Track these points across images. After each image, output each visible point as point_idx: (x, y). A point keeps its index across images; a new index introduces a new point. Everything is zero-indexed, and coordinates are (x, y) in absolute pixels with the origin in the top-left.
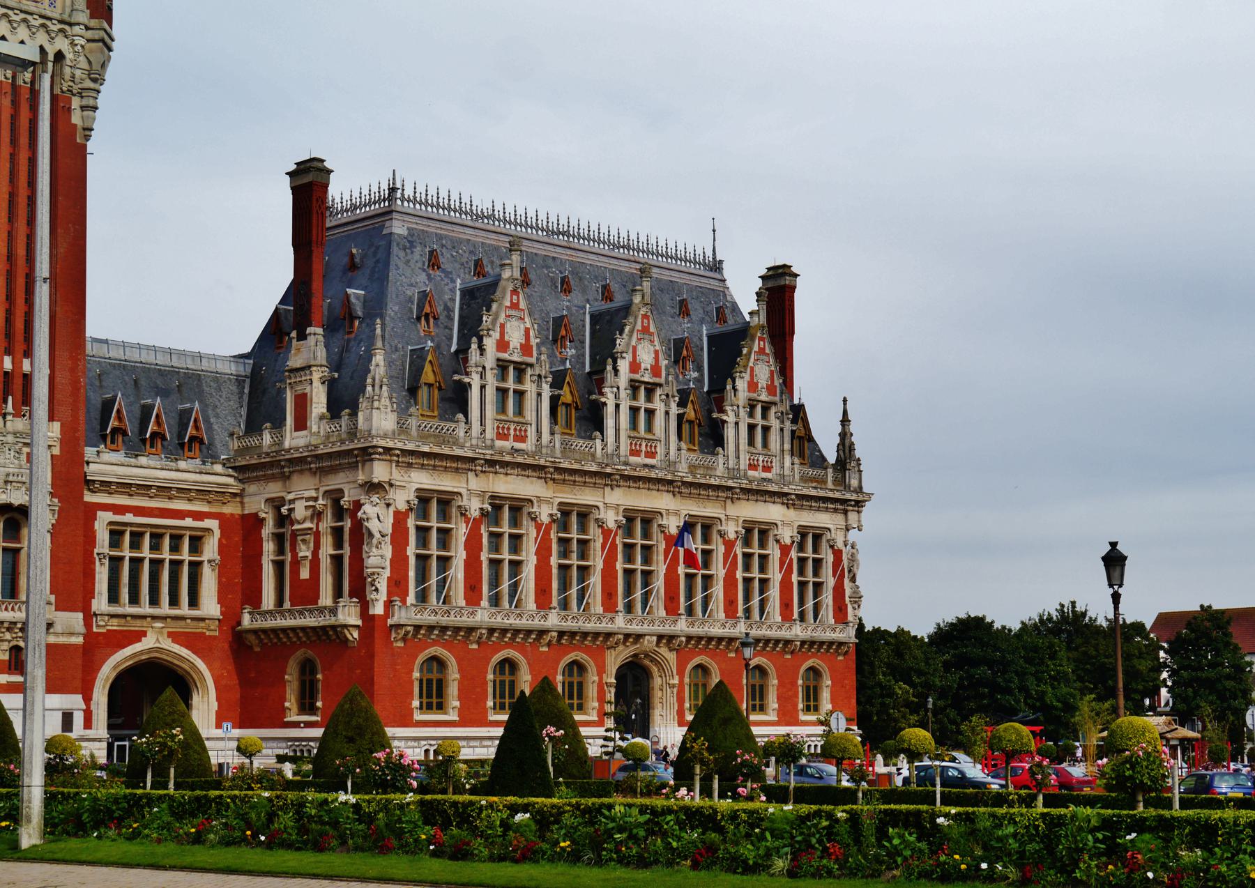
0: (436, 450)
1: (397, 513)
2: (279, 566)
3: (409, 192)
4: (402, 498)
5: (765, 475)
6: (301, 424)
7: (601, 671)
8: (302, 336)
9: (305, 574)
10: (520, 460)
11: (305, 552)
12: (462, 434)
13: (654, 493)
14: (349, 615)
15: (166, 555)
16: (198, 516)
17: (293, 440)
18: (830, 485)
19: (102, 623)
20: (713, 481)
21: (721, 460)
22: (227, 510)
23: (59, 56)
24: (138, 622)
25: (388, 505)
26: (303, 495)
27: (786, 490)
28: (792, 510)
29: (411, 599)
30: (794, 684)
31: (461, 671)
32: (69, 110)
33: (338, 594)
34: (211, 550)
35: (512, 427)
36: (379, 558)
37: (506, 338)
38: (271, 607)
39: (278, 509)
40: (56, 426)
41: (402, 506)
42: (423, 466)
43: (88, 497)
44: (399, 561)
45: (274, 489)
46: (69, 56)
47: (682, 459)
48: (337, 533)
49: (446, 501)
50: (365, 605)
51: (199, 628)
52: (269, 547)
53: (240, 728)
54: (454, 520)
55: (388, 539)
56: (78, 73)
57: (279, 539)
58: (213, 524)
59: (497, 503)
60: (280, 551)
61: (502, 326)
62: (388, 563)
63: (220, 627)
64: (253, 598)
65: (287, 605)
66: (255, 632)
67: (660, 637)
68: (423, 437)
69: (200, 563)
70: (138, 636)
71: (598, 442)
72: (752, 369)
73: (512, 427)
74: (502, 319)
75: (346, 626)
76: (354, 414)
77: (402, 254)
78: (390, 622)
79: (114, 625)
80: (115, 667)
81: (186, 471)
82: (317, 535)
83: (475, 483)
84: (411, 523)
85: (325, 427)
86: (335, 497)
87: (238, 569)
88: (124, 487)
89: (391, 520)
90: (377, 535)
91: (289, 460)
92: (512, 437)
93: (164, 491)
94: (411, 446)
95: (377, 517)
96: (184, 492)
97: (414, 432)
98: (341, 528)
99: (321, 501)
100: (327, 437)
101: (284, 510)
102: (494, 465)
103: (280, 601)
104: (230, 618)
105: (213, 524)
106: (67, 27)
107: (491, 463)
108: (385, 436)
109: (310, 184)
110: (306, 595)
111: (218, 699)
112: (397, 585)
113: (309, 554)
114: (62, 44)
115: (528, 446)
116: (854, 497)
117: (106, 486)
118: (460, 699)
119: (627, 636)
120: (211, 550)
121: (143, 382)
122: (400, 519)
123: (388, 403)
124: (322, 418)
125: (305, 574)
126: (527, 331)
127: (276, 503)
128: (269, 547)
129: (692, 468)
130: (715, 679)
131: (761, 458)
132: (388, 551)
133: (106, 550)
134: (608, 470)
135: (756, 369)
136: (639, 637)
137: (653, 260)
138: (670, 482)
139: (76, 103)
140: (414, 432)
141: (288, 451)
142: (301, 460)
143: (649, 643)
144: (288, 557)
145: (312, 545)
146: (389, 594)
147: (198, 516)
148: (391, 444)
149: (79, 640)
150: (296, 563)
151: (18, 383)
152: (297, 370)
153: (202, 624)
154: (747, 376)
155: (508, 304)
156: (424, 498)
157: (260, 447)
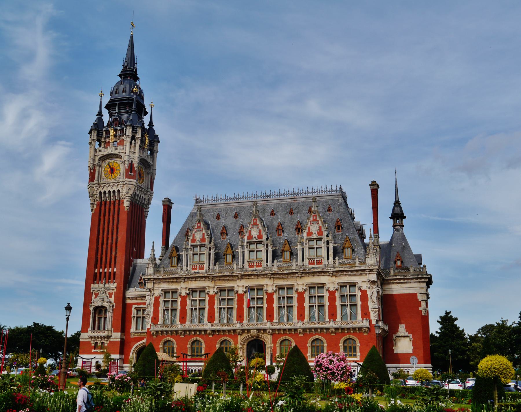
1: (155, 297)
3: (201, 198)
4: (157, 293)
5: (318, 266)
7: (236, 343)
10: (197, 276)
13: (260, 279)
20: (285, 272)
21: (294, 264)
23: (119, 191)
24: (143, 334)
27: (325, 270)
28: (334, 277)
30: (337, 345)
31: (177, 344)
32: (123, 203)
35: (198, 265)
40: (115, 285)
42: (164, 282)
43: (129, 301)
46: (121, 190)
49: (174, 291)
55: (152, 305)
59: (193, 290)
61: (194, 235)
62: (152, 313)
67: (259, 330)
72: (309, 228)
73: (198, 265)
79: (136, 335)
84: (161, 300)
88: (137, 298)
89: (153, 299)
97: (162, 272)
102: (187, 279)
112: (155, 320)
114: (119, 188)
116: (367, 268)
119: (243, 331)
122: (157, 299)
126: (203, 234)
129: (280, 268)
130: (294, 345)
131: (315, 260)
133: (136, 316)
135: (312, 227)
136: (249, 331)
137: (255, 199)
138: (266, 274)
139: (125, 200)
140: (162, 272)
143: (254, 332)
148: (149, 277)
149: (119, 340)
151: (98, 275)
154: (307, 231)
155: (196, 227)
156: (166, 292)
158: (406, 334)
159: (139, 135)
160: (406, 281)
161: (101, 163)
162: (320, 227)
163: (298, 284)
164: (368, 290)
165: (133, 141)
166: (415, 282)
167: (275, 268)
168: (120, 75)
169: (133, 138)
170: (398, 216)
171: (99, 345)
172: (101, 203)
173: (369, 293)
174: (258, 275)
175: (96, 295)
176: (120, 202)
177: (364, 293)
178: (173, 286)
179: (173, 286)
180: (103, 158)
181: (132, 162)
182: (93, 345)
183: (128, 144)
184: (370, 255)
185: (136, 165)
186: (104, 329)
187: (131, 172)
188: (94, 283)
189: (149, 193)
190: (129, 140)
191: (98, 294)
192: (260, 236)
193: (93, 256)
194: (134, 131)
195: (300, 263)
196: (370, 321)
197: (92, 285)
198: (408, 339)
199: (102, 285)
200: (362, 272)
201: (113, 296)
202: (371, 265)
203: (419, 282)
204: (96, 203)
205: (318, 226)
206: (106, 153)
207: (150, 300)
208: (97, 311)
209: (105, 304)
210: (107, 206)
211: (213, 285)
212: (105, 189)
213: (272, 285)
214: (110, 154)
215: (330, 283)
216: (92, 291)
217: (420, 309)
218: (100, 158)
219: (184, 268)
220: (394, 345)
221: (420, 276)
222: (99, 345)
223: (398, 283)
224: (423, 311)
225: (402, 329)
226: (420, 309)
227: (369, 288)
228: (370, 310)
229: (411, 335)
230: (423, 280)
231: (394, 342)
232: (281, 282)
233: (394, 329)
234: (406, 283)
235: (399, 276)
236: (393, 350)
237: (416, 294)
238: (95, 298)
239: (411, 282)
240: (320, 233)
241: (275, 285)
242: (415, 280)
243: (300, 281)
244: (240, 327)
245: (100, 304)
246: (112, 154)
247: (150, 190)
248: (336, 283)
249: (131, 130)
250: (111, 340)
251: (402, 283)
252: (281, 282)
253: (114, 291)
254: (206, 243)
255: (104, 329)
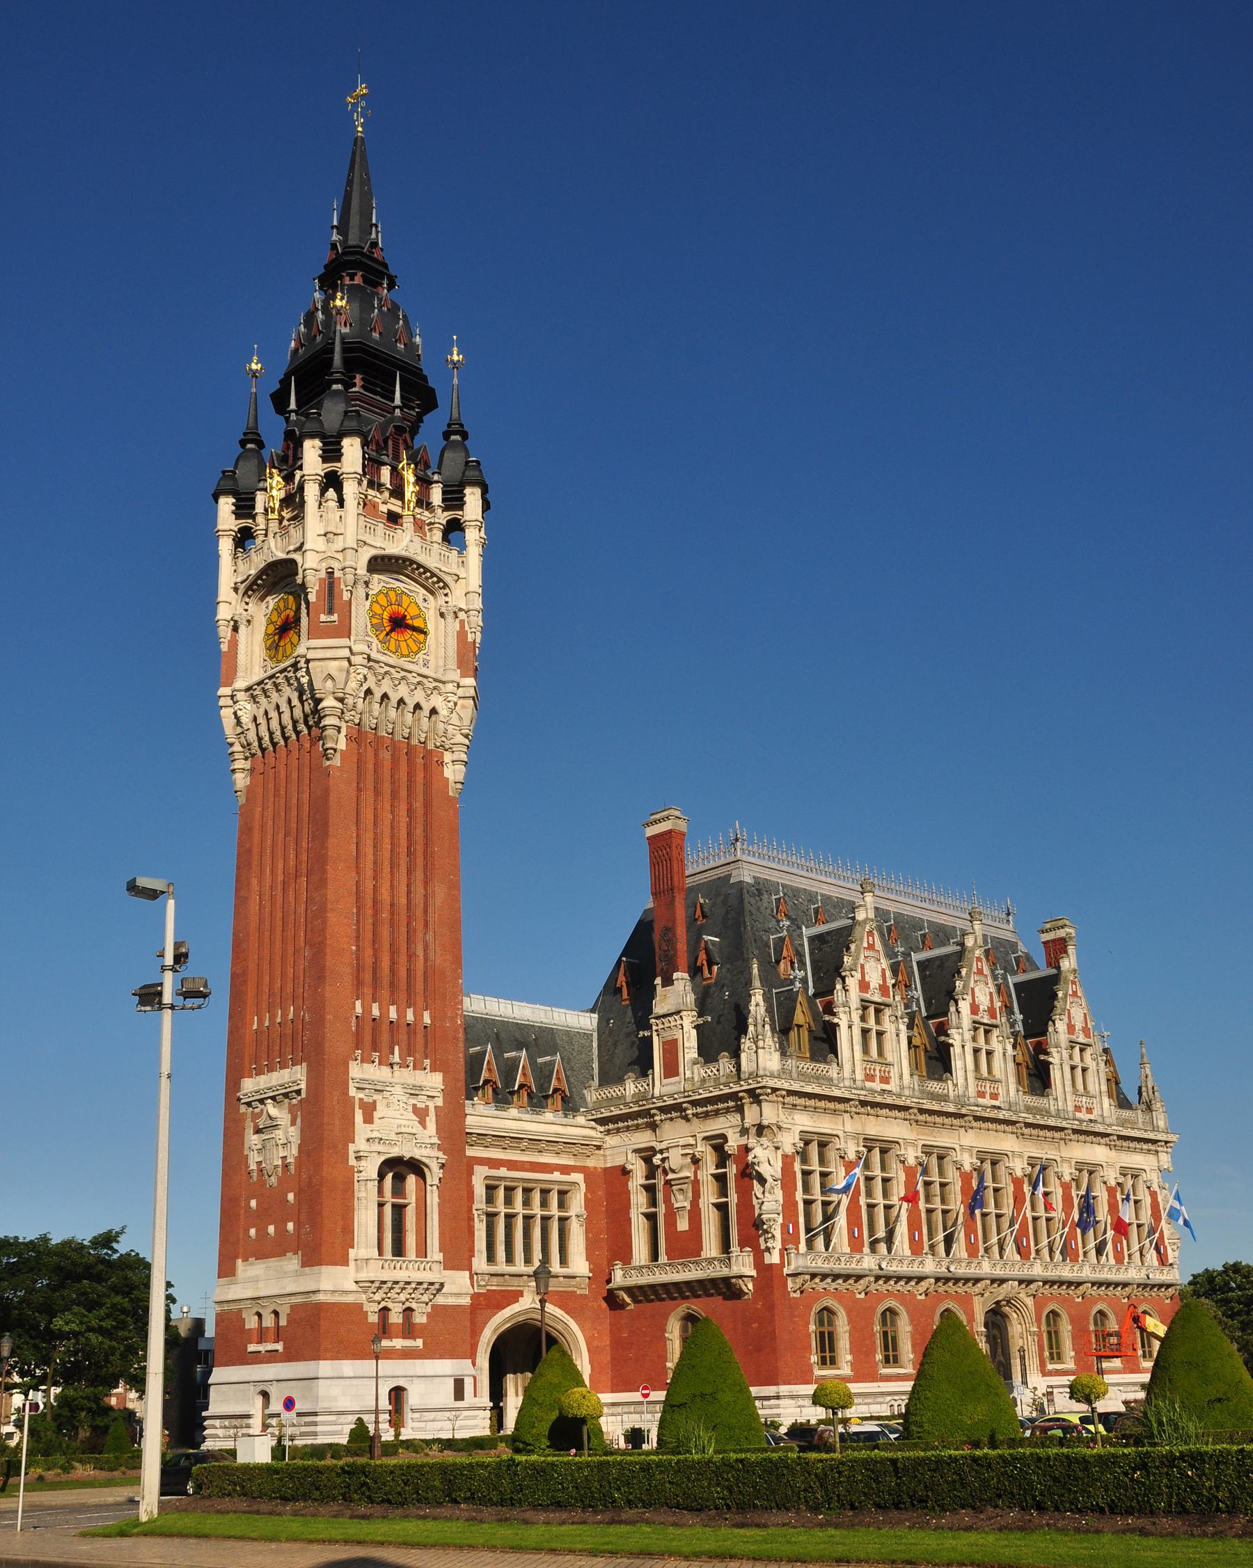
0: (808, 1089)
1: (785, 1156)
2: (651, 1218)
6: (671, 1069)
8: (668, 982)
9: (683, 1225)
10: (889, 1101)
11: (682, 1201)
12: (835, 1075)
14: (743, 1265)
15: (537, 1210)
16: (565, 1170)
17: (661, 1087)
19: (483, 1283)
22: (590, 1163)
24: (515, 1281)
25: (777, 1148)
26: (679, 1141)
29: (803, 1247)
33: (726, 1246)
34: (577, 1204)
35: (878, 1068)
36: (770, 1202)
37: (867, 979)
38: (643, 1263)
39: (648, 1161)
41: (789, 1150)
45: (643, 1139)
46: (443, 712)
48: (721, 1179)
50: (759, 1255)
51: (570, 1286)
52: (639, 1201)
53: (612, 1392)
54: (833, 1164)
56: (450, 728)
57: (650, 1189)
58: (578, 1177)
60: (653, 1202)
63: (590, 1285)
64: (623, 1252)
65: (663, 1258)
66: (629, 1290)
68: (803, 1076)
69: (567, 1218)
70: (515, 1296)
73: (878, 1068)
74: (862, 961)
75: (741, 1277)
76: (736, 1054)
77: (752, 900)
78: (786, 1271)
80: (496, 1330)
81: (548, 1124)
82: (696, 1184)
84: (797, 1167)
85: (700, 1072)
86: (718, 1144)
87: (603, 1223)
88: (499, 1140)
89: (779, 1164)
90: (770, 1180)
91: (659, 1108)
92: (878, 1079)
93: (535, 1143)
94: (796, 1087)
95: (768, 1161)
96: (552, 1144)
98: (725, 1174)
99: (699, 1149)
100: (703, 1080)
101: (656, 1160)
103: (654, 1256)
104: (601, 1275)
105: (578, 1177)
106: (440, 685)
107: (864, 1103)
108: (772, 1076)
109: (670, 832)
110: (687, 1246)
111: (591, 1362)
113: (687, 1205)
114: (437, 701)
115: (893, 1086)
117: (482, 1138)
118: (852, 1352)
120: (577, 1204)
121: (503, 1035)
122: (787, 1161)
123: (771, 1043)
124: (695, 1063)
125: (683, 1225)
126: (883, 970)
127: (647, 1155)
128: (639, 1201)
132: (779, 1194)
133: (483, 1206)
134: (964, 1111)
138: (1013, 1123)
139: (448, 757)
141: (661, 1097)
142: (678, 1107)
143: (1009, 1288)
144: (661, 1209)
145: (690, 1194)
146: (784, 1242)
147: (565, 1170)
150: (671, 1215)
152: (664, 1016)
153: (573, 1282)
155: (865, 945)
157: (623, 1097)
171: (396, 1318)
175: (369, 1112)
178: (824, 1125)
179: (824, 1125)
180: (380, 564)
182: (373, 1318)
191: (373, 1106)
197: (352, 1064)
201: (431, 1122)
206: (393, 549)
209: (418, 1153)
214: (405, 559)
216: (352, 1092)
222: (396, 1318)
238: (368, 1119)
246: (412, 562)
250: (440, 1300)
253: (431, 1105)
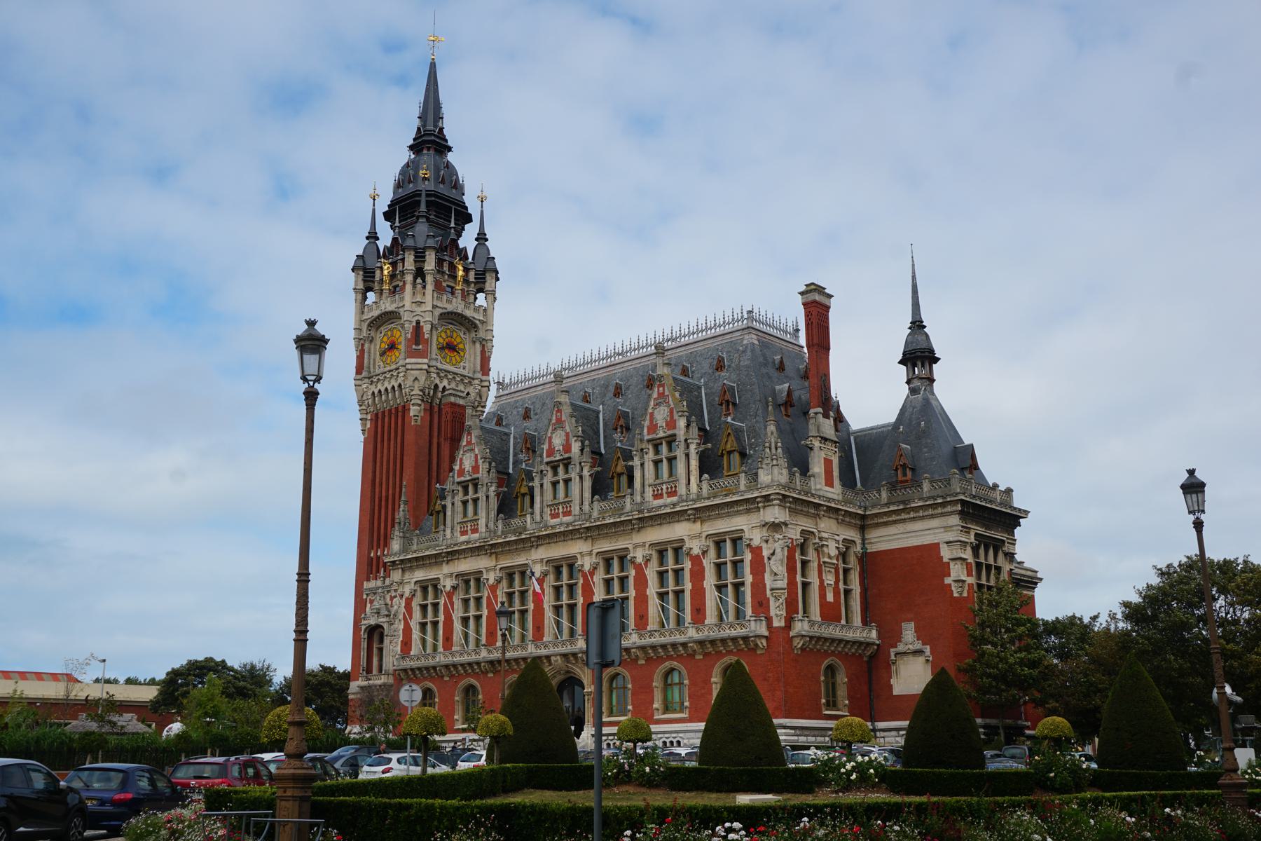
4: (407, 590)
18: (742, 488)
21: (628, 500)
23: (400, 386)
42: (418, 567)
44: (407, 631)
47: (597, 511)
71: (528, 517)
72: (652, 414)
83: (446, 569)
102: (452, 555)
114: (400, 380)
126: (476, 456)
156: (424, 587)
158: (918, 645)
159: (430, 264)
160: (912, 515)
161: (373, 333)
162: (671, 411)
163: (635, 547)
164: (764, 545)
165: (419, 280)
166: (932, 516)
167: (595, 514)
168: (411, 148)
169: (420, 273)
170: (919, 357)
172: (377, 415)
173: (766, 553)
174: (564, 533)
175: (371, 602)
176: (405, 409)
177: (756, 551)
178: (431, 574)
179: (431, 574)
181: (418, 322)
183: (409, 287)
184: (766, 461)
185: (426, 328)
186: (380, 670)
187: (417, 344)
188: (368, 580)
189: (477, 382)
190: (409, 278)
192: (567, 448)
193: (367, 526)
194: (420, 256)
195: (638, 498)
196: (769, 620)
198: (921, 659)
199: (379, 583)
200: (750, 505)
202: (768, 486)
203: (942, 515)
204: (369, 417)
205: (666, 409)
207: (399, 605)
208: (376, 638)
210: (386, 419)
211: (493, 563)
212: (379, 386)
213: (590, 553)
215: (691, 537)
217: (948, 581)
218: (369, 325)
219: (448, 531)
220: (894, 675)
221: (940, 501)
223: (895, 522)
224: (953, 584)
225: (909, 632)
226: (948, 581)
227: (767, 541)
228: (768, 592)
229: (927, 649)
230: (949, 509)
231: (893, 668)
232: (606, 545)
233: (891, 636)
234: (913, 519)
235: (894, 504)
236: (891, 687)
237: (938, 544)
239: (923, 518)
240: (671, 424)
241: (595, 551)
242: (930, 512)
243: (638, 538)
244: (534, 650)
245: (372, 621)
247: (479, 375)
248: (704, 535)
249: (412, 257)
251: (904, 520)
252: (606, 545)
254: (479, 475)
255: (380, 670)
